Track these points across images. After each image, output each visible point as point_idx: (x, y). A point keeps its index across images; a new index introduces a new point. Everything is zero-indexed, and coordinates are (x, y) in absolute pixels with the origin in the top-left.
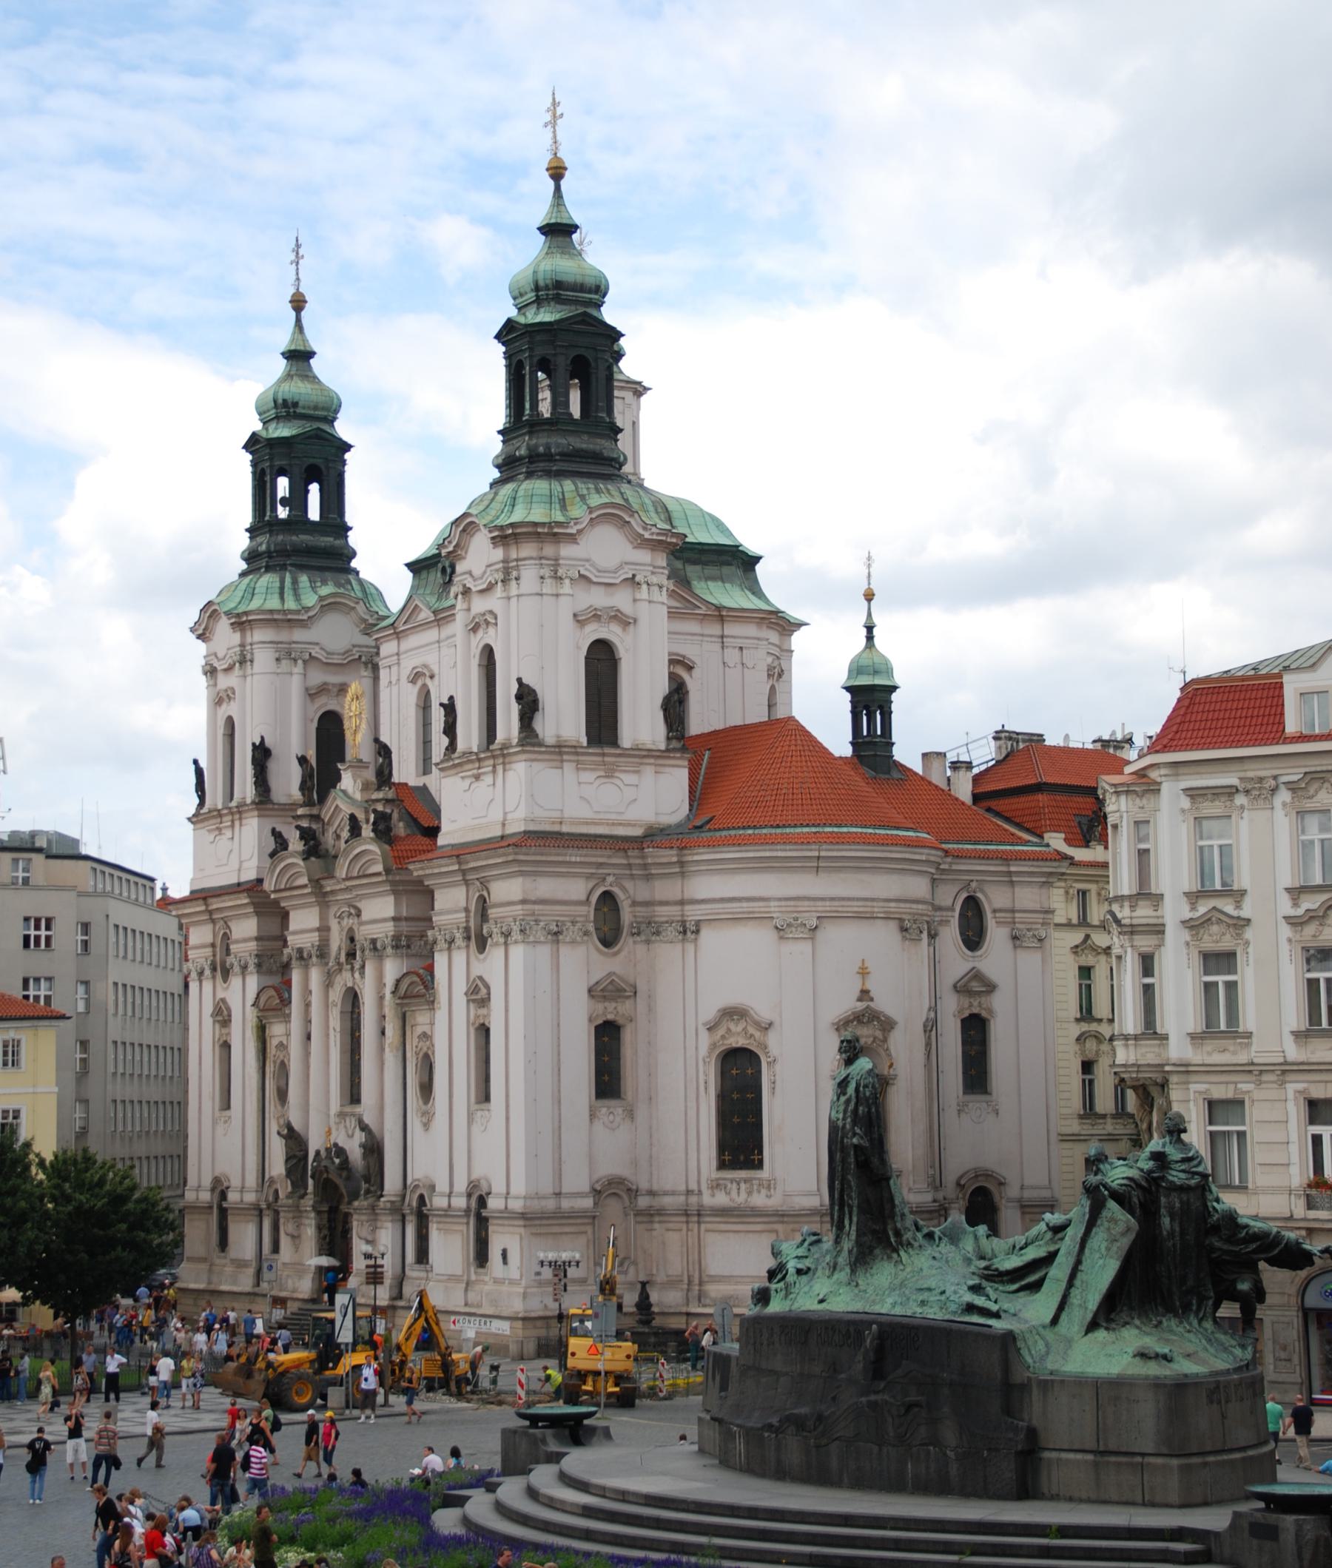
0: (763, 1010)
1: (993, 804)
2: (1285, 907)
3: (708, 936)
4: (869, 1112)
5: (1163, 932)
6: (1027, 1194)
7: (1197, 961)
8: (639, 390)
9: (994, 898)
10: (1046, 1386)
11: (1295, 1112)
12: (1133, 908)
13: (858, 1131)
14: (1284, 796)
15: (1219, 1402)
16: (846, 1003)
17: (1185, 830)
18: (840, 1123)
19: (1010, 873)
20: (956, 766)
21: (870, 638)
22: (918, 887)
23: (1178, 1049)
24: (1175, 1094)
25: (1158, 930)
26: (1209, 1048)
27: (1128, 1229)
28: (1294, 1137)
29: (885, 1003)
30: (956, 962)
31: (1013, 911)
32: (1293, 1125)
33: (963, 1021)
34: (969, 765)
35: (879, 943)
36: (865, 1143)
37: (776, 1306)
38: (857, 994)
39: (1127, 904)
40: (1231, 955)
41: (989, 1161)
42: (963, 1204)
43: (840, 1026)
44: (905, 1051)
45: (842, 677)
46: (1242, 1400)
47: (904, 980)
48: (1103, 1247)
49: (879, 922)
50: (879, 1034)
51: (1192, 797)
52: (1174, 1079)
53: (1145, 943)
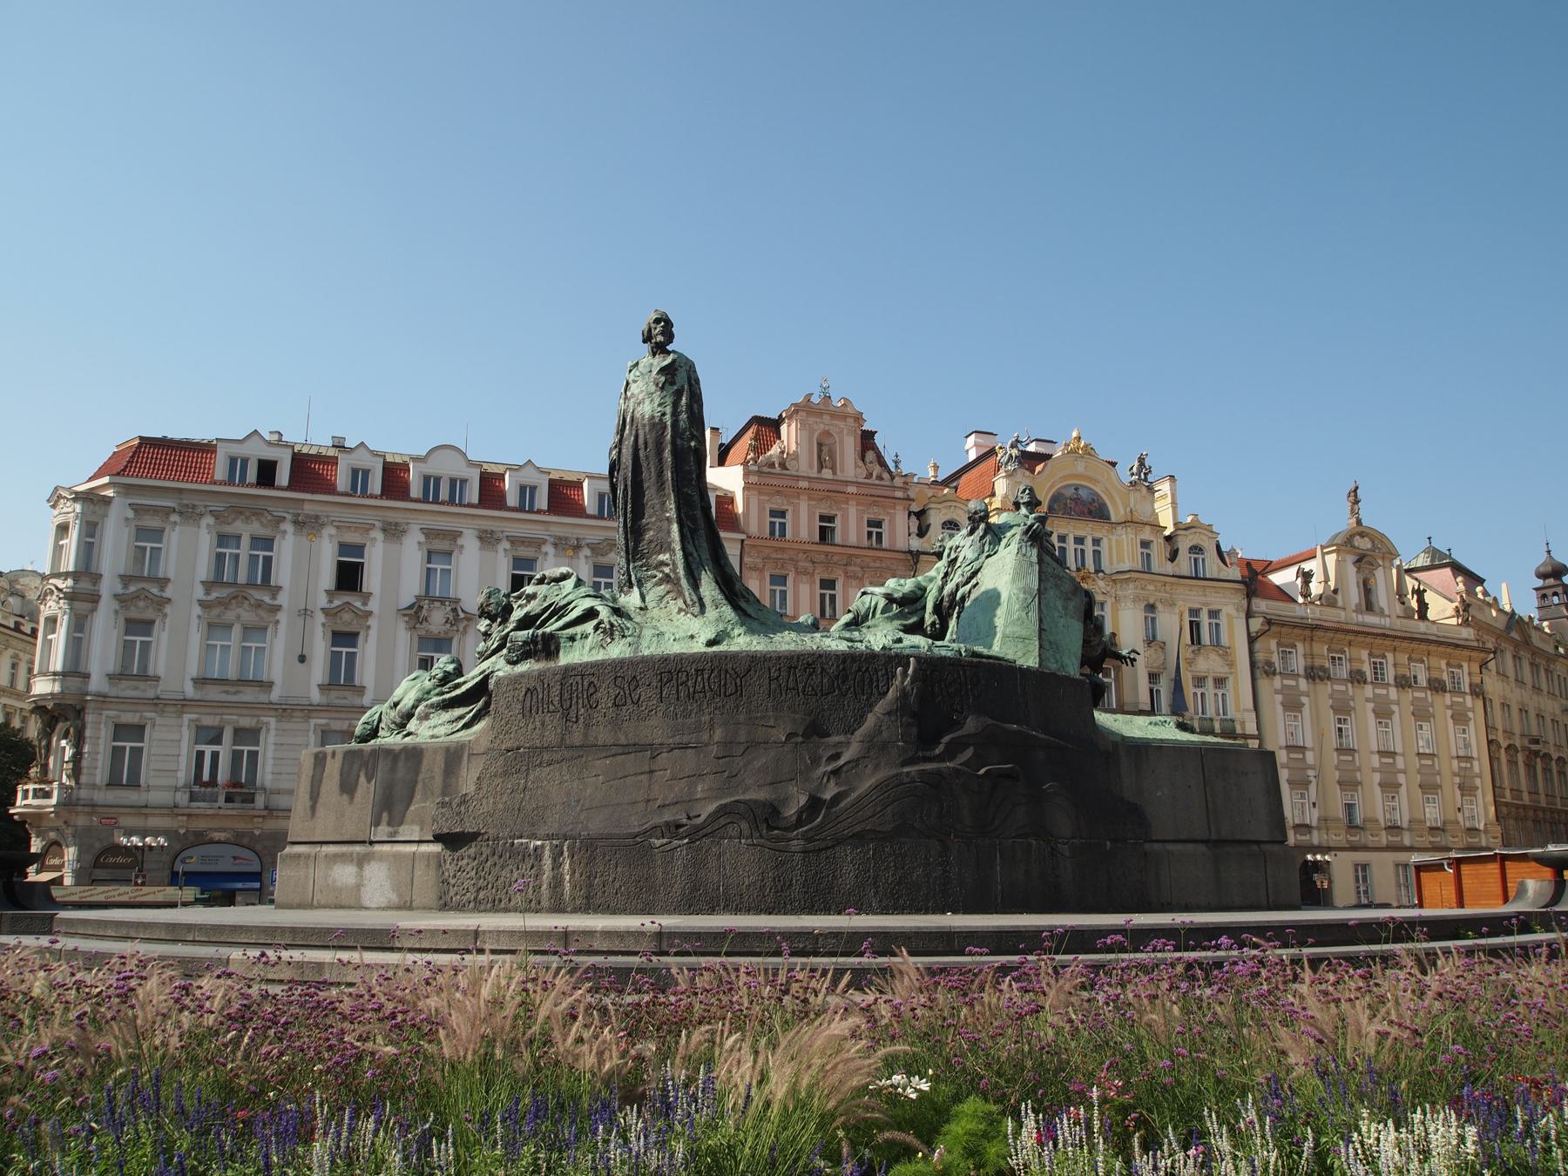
2: (199, 592)
10: (1141, 749)
11: (186, 735)
14: (209, 520)
17: (127, 534)
18: (668, 419)
24: (90, 718)
25: (94, 599)
28: (184, 751)
32: (185, 745)
37: (570, 656)
40: (152, 622)
48: (1059, 604)
51: (136, 511)
52: (90, 706)
53: (82, 606)
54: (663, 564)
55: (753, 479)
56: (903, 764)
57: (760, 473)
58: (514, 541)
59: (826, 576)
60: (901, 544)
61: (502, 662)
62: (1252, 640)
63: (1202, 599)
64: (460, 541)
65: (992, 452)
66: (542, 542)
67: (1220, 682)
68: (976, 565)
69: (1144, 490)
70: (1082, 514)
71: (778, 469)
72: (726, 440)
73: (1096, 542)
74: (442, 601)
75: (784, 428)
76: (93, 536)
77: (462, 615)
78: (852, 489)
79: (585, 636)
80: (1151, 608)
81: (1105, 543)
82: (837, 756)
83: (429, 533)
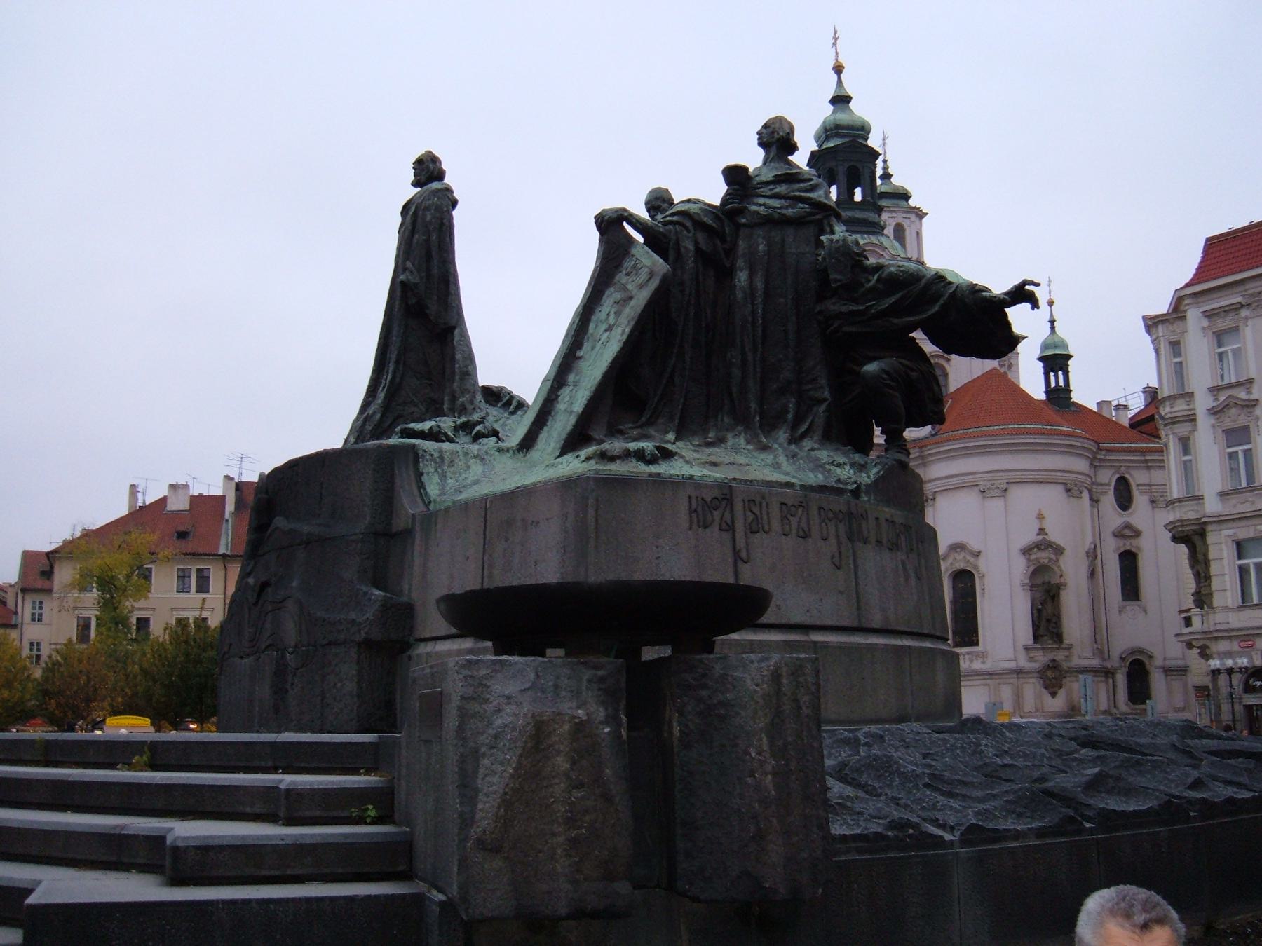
0: (974, 544)
1: (1143, 428)
3: (939, 498)
4: (428, 241)
5: (1194, 420)
6: (1168, 663)
7: (1221, 436)
8: (920, 214)
9: (1137, 478)
10: (430, 519)
12: (1172, 406)
13: (409, 264)
15: (730, 528)
16: (1030, 537)
19: (1147, 461)
20: (1117, 407)
21: (1053, 328)
22: (1081, 465)
23: (1212, 506)
24: (1211, 538)
25: (1191, 419)
26: (1234, 502)
27: (651, 275)
29: (1055, 536)
30: (1113, 517)
31: (1150, 485)
33: (1121, 555)
34: (1126, 407)
35: (1050, 500)
36: (414, 279)
38: (1037, 531)
39: (1167, 403)
40: (1246, 430)
41: (1141, 641)
42: (1125, 670)
43: (1026, 551)
44: (1073, 571)
45: (1037, 354)
46: (805, 536)
47: (1070, 523)
49: (1052, 487)
50: (1053, 557)
52: (1209, 528)
53: (1182, 429)
76: (1180, 355)
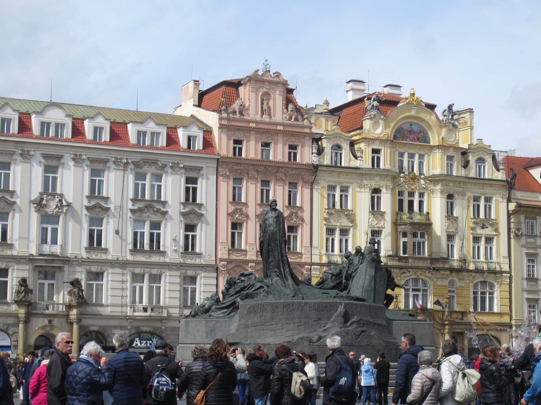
54: (276, 272)
55: (224, 122)
56: (341, 328)
57: (228, 119)
58: (92, 160)
59: (264, 179)
60: (306, 161)
61: (239, 300)
62: (509, 215)
63: (482, 191)
64: (62, 161)
65: (361, 100)
66: (106, 162)
67: (489, 240)
68: (357, 266)
69: (451, 126)
70: (414, 140)
71: (238, 116)
72: (204, 87)
73: (421, 156)
74: (54, 195)
75: (241, 89)
77: (65, 203)
78: (280, 128)
79: (261, 293)
80: (450, 197)
81: (426, 157)
82: (324, 326)
83: (46, 157)
